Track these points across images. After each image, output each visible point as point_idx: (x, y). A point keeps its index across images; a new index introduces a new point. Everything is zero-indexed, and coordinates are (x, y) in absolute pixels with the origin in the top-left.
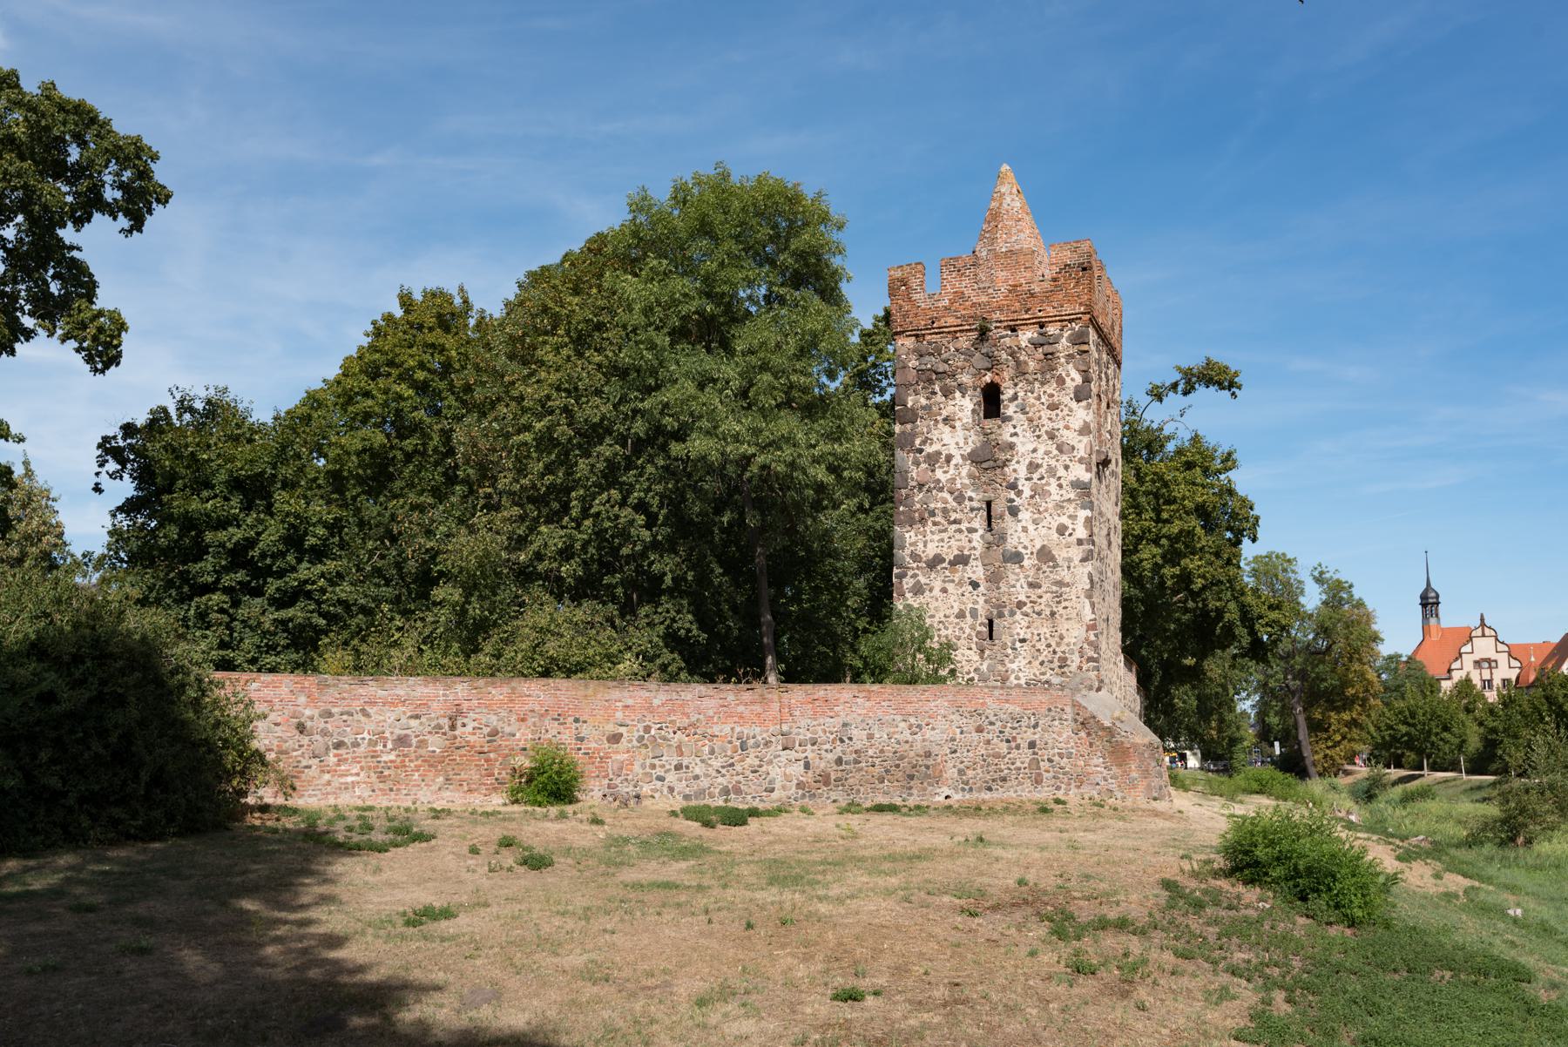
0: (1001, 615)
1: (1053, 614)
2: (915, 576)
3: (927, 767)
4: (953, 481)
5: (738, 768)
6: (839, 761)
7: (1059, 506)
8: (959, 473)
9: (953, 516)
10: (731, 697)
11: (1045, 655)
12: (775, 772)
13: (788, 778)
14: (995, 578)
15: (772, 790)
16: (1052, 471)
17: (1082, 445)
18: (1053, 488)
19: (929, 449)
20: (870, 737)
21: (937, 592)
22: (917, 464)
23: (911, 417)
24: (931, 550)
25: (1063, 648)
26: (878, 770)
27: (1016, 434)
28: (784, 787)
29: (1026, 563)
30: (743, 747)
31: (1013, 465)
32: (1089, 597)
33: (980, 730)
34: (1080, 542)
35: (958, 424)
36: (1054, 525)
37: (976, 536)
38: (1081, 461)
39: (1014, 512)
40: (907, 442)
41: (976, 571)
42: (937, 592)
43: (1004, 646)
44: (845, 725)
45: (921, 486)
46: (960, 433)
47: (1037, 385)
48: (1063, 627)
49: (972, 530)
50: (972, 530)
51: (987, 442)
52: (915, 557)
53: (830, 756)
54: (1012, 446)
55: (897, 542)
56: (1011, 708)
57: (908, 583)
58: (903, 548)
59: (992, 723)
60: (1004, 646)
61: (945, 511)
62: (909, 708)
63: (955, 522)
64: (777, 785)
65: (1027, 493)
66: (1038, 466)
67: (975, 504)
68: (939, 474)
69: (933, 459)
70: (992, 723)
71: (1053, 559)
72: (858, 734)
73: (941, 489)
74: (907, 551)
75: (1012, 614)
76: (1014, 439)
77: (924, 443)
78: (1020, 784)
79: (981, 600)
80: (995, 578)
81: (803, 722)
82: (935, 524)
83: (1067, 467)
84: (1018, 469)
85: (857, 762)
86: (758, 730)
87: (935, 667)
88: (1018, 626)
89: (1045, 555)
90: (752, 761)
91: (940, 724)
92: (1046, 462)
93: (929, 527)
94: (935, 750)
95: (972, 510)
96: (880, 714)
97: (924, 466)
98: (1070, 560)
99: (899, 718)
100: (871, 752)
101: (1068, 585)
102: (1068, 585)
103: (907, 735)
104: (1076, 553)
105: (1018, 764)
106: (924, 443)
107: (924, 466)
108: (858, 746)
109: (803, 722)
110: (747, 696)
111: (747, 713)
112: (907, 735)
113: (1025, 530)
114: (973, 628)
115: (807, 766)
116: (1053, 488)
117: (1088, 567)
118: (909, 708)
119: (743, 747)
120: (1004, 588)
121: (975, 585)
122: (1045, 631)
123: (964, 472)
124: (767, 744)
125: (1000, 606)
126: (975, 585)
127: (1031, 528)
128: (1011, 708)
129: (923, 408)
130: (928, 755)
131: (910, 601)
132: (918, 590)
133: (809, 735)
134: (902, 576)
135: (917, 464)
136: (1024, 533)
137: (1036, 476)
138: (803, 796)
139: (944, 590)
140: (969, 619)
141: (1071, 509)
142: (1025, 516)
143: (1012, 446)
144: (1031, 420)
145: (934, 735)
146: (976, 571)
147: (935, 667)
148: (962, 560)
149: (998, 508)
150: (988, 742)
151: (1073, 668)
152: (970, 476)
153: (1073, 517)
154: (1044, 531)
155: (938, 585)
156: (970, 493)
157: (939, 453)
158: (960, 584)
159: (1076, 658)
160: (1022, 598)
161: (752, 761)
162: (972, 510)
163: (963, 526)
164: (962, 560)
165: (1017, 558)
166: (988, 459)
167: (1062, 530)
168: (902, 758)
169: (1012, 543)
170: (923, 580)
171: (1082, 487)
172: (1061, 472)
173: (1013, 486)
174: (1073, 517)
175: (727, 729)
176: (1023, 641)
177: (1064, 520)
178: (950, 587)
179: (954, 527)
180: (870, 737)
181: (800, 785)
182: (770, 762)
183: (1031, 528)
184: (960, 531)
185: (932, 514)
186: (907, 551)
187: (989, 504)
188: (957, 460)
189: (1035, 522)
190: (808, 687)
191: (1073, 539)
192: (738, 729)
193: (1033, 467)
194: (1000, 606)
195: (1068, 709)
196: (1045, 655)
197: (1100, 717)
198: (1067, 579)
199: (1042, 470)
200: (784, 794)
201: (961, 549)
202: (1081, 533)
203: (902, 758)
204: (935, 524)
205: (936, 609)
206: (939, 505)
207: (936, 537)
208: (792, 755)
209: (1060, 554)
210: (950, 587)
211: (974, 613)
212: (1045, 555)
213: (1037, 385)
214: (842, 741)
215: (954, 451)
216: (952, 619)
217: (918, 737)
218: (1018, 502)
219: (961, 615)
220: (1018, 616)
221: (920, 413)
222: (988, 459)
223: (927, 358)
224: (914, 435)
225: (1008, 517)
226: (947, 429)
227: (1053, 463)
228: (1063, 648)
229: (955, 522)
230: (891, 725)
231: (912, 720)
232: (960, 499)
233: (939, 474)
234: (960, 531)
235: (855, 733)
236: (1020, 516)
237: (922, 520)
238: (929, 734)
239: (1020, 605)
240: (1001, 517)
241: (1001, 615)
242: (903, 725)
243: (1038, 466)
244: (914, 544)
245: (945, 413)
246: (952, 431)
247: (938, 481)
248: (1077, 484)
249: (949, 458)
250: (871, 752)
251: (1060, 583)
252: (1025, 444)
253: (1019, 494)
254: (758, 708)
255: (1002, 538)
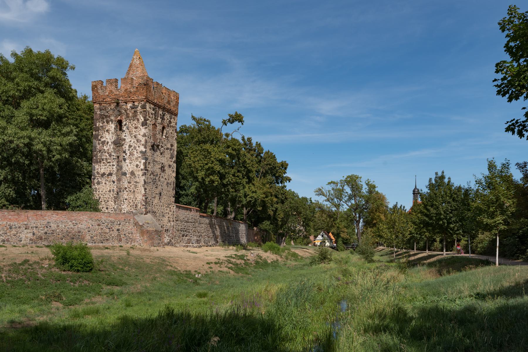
0: (120, 191)
1: (134, 191)
2: (98, 179)
3: (79, 236)
4: (108, 150)
5: (8, 234)
6: (46, 233)
7: (137, 159)
8: (110, 147)
9: (109, 161)
10: (6, 213)
11: (132, 204)
12: (23, 236)
13: (27, 237)
14: (119, 180)
15: (21, 241)
16: (135, 148)
17: (143, 140)
18: (135, 153)
19: (102, 140)
20: (58, 226)
21: (103, 184)
22: (99, 144)
23: (97, 129)
24: (102, 171)
25: (137, 202)
26: (60, 236)
27: (125, 136)
28: (25, 240)
29: (127, 176)
30: (11, 228)
31: (125, 146)
32: (143, 186)
33: (99, 225)
34: (142, 170)
35: (110, 132)
36: (135, 165)
37: (114, 167)
38: (143, 145)
39: (125, 160)
40: (96, 137)
41: (114, 178)
42: (103, 184)
43: (121, 201)
44: (48, 222)
45: (100, 151)
46: (111, 135)
47: (132, 121)
48: (137, 195)
49: (113, 165)
50: (113, 165)
51: (118, 138)
52: (98, 173)
53: (42, 231)
54: (125, 140)
55: (93, 168)
56: (111, 219)
57: (96, 181)
58: (95, 170)
59: (103, 223)
60: (121, 201)
61: (106, 159)
62: (73, 218)
63: (109, 162)
64: (23, 240)
65: (128, 154)
66: (131, 146)
67: (114, 157)
68: (105, 148)
69: (103, 143)
70: (103, 223)
71: (134, 175)
72: (54, 226)
73: (105, 152)
74: (96, 171)
75: (123, 191)
76: (125, 138)
77: (101, 138)
78: (113, 241)
79: (115, 187)
80: (119, 180)
81: (33, 221)
82: (104, 163)
83: (139, 147)
84: (126, 147)
85: (52, 233)
86: (16, 223)
87: (92, 206)
88: (125, 195)
89: (132, 173)
90: (13, 232)
91: (84, 223)
92: (133, 145)
93: (102, 164)
94: (82, 231)
95: (114, 159)
96: (62, 219)
97: (101, 145)
98: (139, 175)
99: (69, 221)
100: (58, 231)
101: (138, 183)
102: (138, 183)
103: (72, 226)
104: (141, 173)
105: (113, 235)
106: (101, 138)
107: (101, 145)
108: (53, 229)
109: (33, 221)
110: (12, 213)
111: (12, 218)
112: (72, 226)
113: (127, 165)
114: (113, 195)
115: (34, 234)
116: (135, 153)
117: (144, 178)
118: (73, 218)
119: (11, 228)
120: (121, 183)
121: (114, 182)
122: (132, 196)
123: (112, 147)
124: (19, 227)
125: (120, 189)
126: (114, 182)
127: (129, 165)
128: (111, 219)
129: (101, 127)
130: (79, 232)
131: (96, 187)
132: (99, 183)
133: (35, 225)
134: (94, 179)
135: (99, 144)
136: (128, 167)
137: (131, 149)
138: (32, 243)
139: (105, 183)
140: (112, 192)
141: (140, 159)
142: (127, 161)
143: (125, 140)
144: (130, 132)
145: (82, 226)
146: (114, 178)
147: (92, 206)
148: (110, 174)
149: (121, 158)
150: (102, 229)
151: (139, 208)
152: (113, 148)
153: (140, 162)
154: (132, 166)
155: (104, 182)
156: (113, 154)
157: (105, 141)
158: (110, 182)
159: (140, 205)
160: (126, 186)
161: (13, 232)
162: (114, 159)
163: (111, 164)
164: (110, 174)
165: (125, 174)
166: (118, 143)
167: (137, 166)
168: (70, 233)
169: (124, 169)
170: (100, 180)
171: (143, 153)
172: (137, 148)
173: (125, 152)
174: (140, 162)
175: (5, 223)
176: (126, 199)
177: (138, 163)
178: (107, 182)
179: (109, 164)
180: (58, 226)
181: (30, 240)
182: (21, 233)
183: (129, 165)
184: (110, 165)
185: (103, 160)
186: (96, 171)
187: (118, 157)
188: (110, 143)
189: (130, 163)
190: (35, 211)
191: (140, 169)
192: (9, 223)
193: (130, 146)
194: (120, 189)
195: (132, 220)
196: (132, 204)
197: (139, 222)
198: (138, 181)
199: (132, 147)
200: (25, 242)
201: (110, 171)
202: (142, 167)
203: (70, 233)
204: (104, 163)
205: (103, 189)
206: (105, 157)
207: (104, 167)
208: (29, 231)
209: (137, 173)
210: (107, 182)
211: (113, 190)
212: (132, 173)
213: (132, 121)
214: (47, 227)
215: (109, 141)
216: (107, 192)
217: (76, 227)
218: (126, 157)
219: (110, 191)
220: (125, 192)
221: (100, 128)
222: (118, 143)
223: (102, 111)
224: (98, 135)
225: (123, 161)
226: (107, 134)
227: (135, 145)
228: (137, 202)
229: (109, 162)
230: (65, 223)
231: (74, 222)
232: (110, 155)
233: (105, 148)
234: (110, 165)
235: (52, 225)
236: (126, 161)
237: (100, 162)
238: (80, 226)
239: (126, 188)
240: (121, 161)
241: (120, 191)
242: (70, 223)
243: (131, 146)
244: (97, 169)
245: (107, 129)
246: (108, 135)
247: (105, 150)
248: (141, 152)
249: (108, 143)
250: (58, 231)
251: (136, 182)
252: (128, 139)
253: (126, 154)
254: (16, 217)
255: (121, 168)
